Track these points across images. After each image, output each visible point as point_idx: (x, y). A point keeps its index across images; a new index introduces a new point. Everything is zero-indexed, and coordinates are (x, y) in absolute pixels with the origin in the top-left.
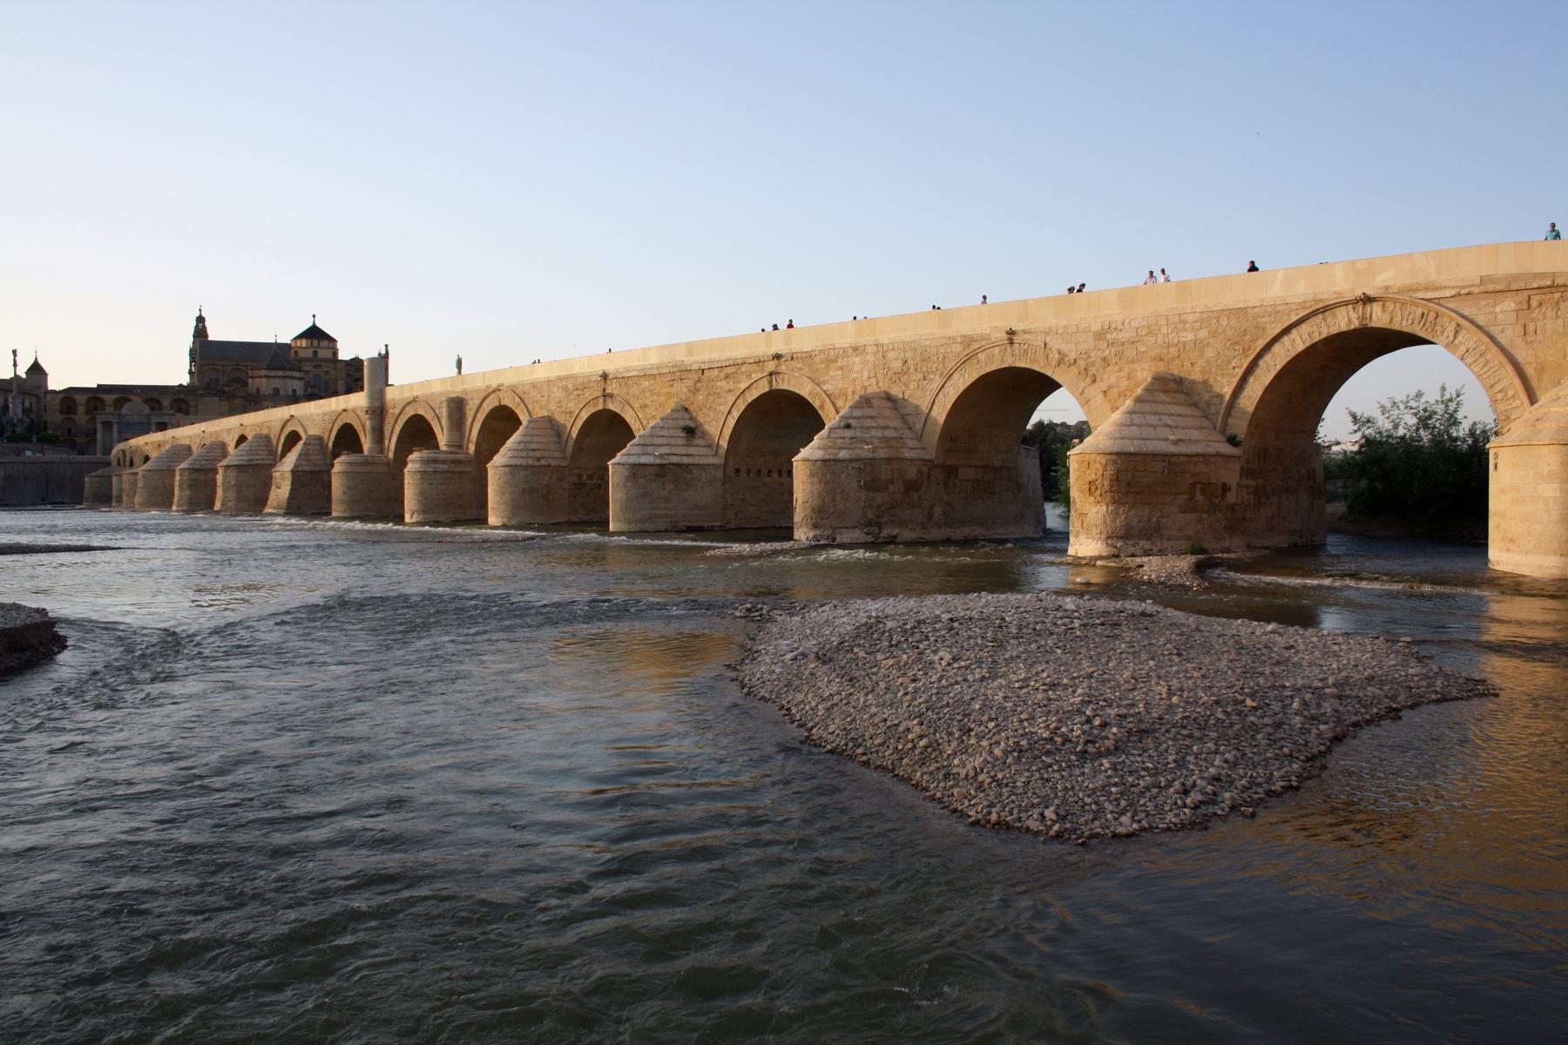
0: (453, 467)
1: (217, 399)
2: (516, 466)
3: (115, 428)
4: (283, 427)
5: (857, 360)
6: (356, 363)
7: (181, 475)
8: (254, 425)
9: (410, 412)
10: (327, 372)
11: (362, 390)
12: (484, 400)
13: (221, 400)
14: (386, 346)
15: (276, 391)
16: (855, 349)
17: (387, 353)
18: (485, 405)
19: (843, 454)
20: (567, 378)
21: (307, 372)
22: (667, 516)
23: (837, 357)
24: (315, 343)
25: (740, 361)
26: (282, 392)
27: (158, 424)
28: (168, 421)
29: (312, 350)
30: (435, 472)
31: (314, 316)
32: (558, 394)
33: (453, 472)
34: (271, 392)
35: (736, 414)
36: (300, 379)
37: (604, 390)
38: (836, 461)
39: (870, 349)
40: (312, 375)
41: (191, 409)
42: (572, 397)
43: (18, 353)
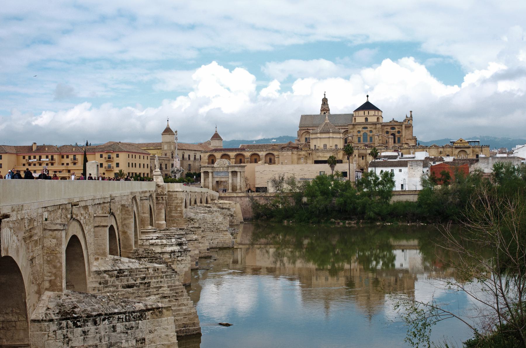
1: (290, 153)
3: (210, 174)
6: (393, 124)
10: (371, 131)
13: (292, 153)
14: (411, 112)
15: (325, 146)
17: (411, 116)
21: (359, 132)
24: (366, 112)
26: (328, 147)
27: (232, 172)
28: (237, 170)
31: (368, 96)
36: (340, 138)
40: (362, 133)
41: (276, 159)
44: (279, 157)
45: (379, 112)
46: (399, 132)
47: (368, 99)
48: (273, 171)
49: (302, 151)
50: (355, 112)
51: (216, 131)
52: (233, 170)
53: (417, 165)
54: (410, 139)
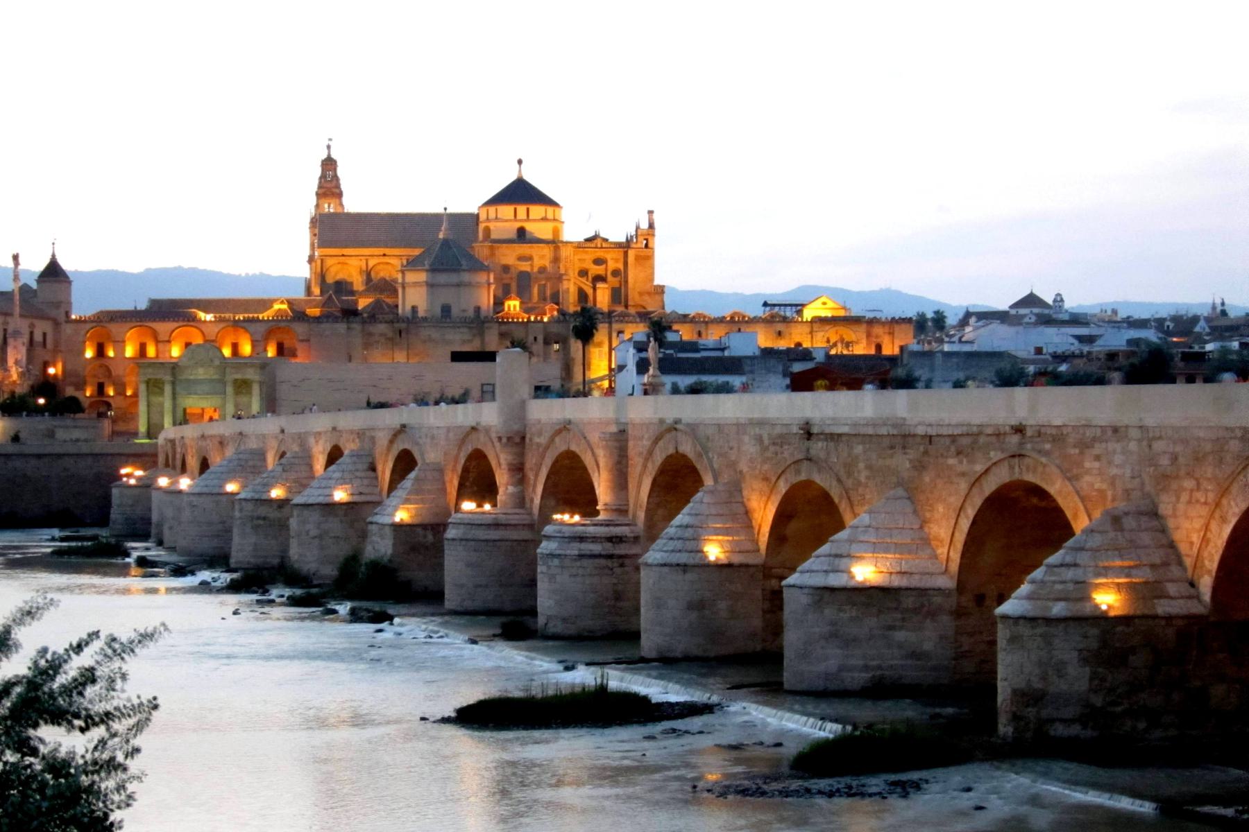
0: (608, 548)
2: (678, 565)
3: (168, 389)
4: (391, 442)
5: (1118, 447)
7: (241, 510)
8: (352, 432)
9: (560, 446)
11: (493, 399)
12: (657, 440)
13: (348, 328)
14: (651, 212)
15: (446, 310)
16: (1116, 430)
17: (651, 226)
18: (657, 451)
19: (1058, 609)
20: (761, 423)
22: (866, 668)
23: (1094, 439)
24: (522, 210)
25: (975, 429)
26: (455, 312)
27: (236, 380)
29: (518, 225)
30: (581, 556)
31: (520, 162)
32: (750, 448)
33: (610, 557)
34: (438, 311)
35: (971, 512)
37: (808, 450)
38: (1049, 621)
39: (1134, 433)
42: (769, 454)
43: (21, 259)
44: (309, 341)
45: (557, 209)
46: (616, 273)
47: (520, 171)
48: (330, 381)
49: (375, 321)
50: (485, 209)
51: (53, 256)
52: (239, 376)
53: (769, 371)
54: (649, 294)
